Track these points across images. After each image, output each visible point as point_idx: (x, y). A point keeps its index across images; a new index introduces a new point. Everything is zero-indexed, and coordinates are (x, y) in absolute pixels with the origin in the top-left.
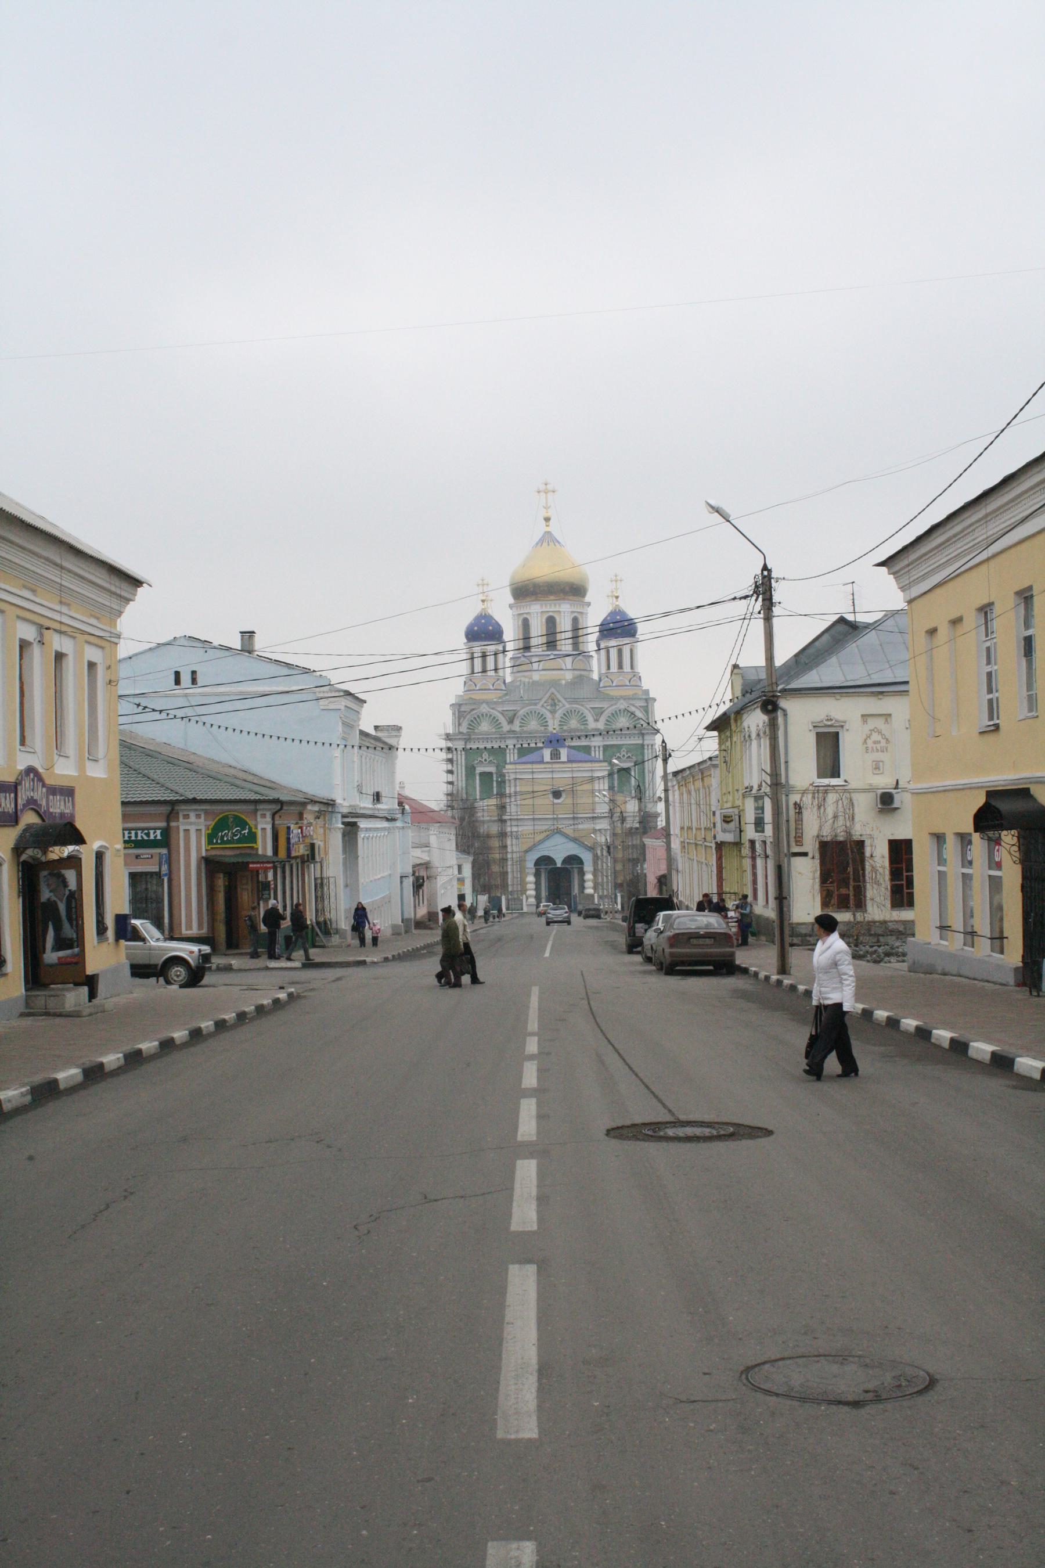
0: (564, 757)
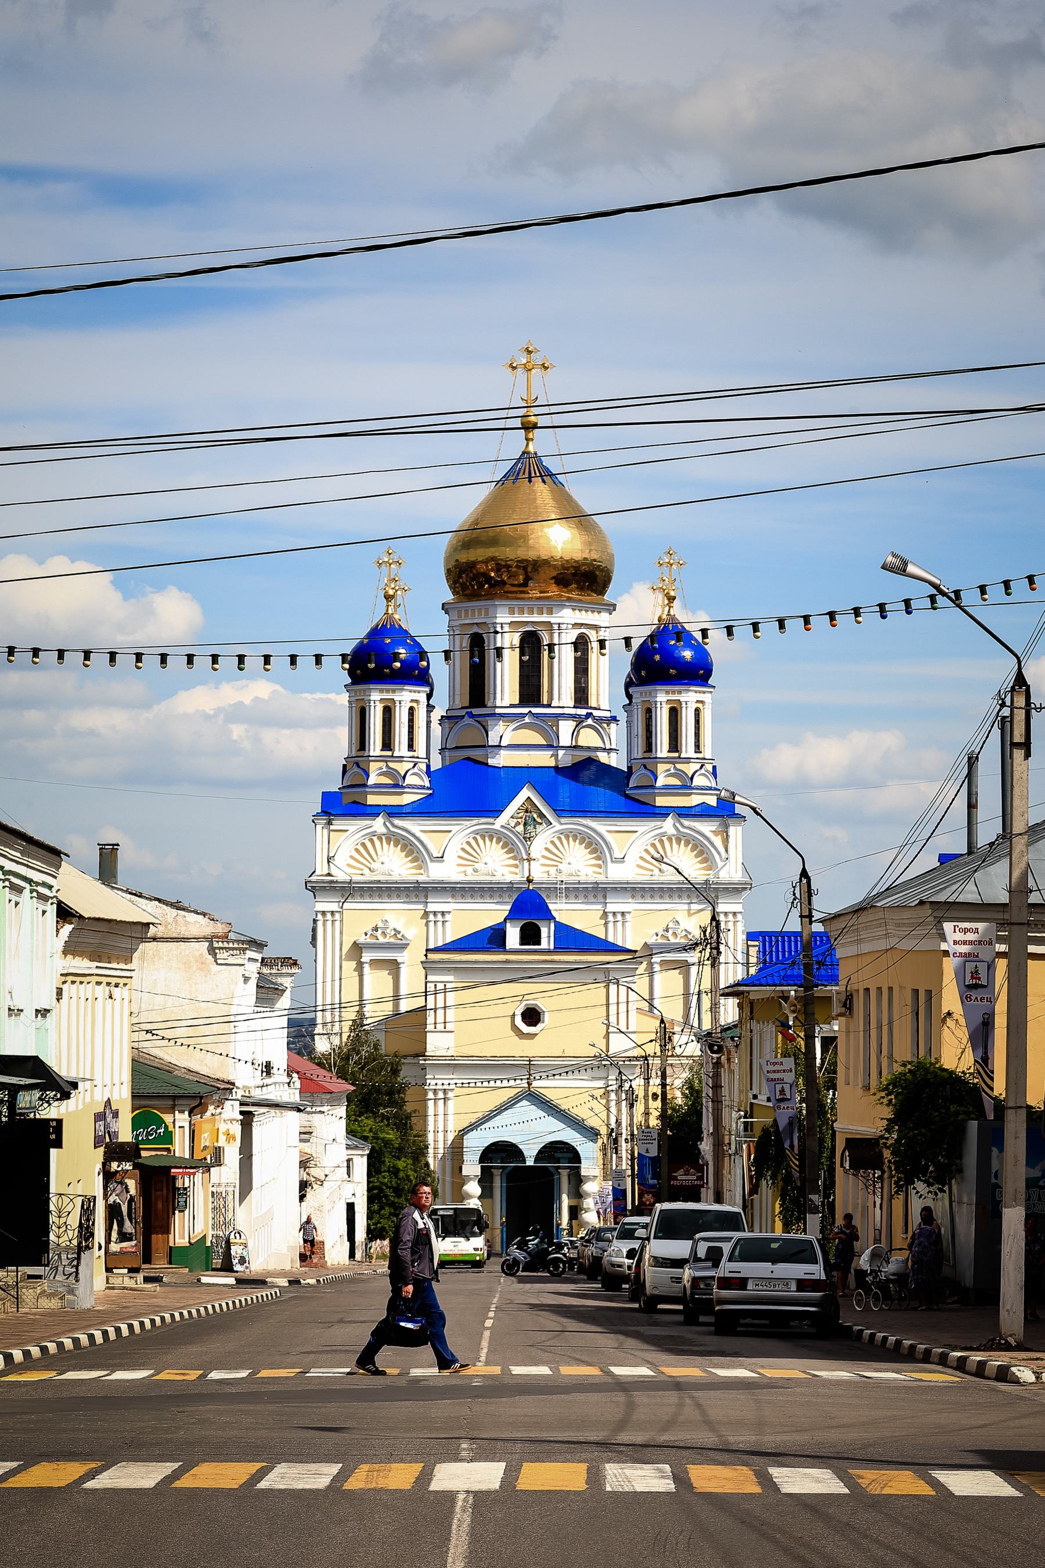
0: (547, 939)
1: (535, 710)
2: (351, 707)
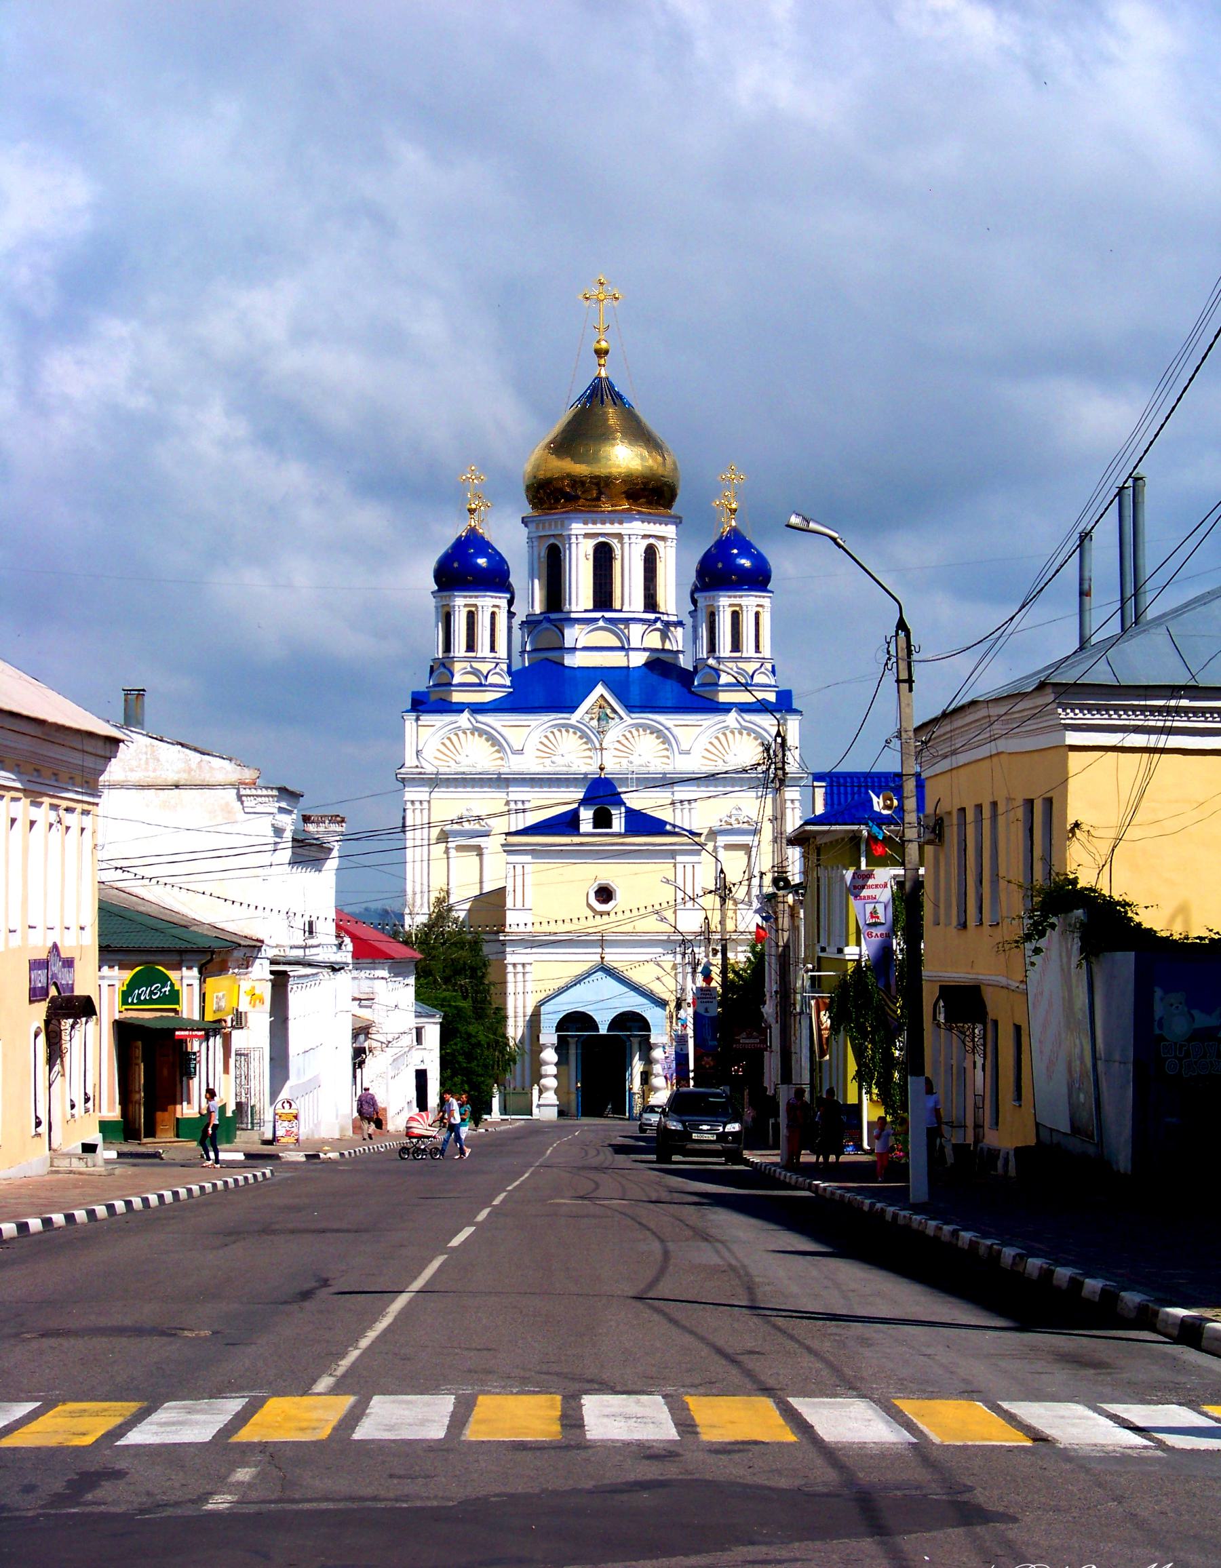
0: (618, 824)
1: (608, 615)
2: (437, 612)
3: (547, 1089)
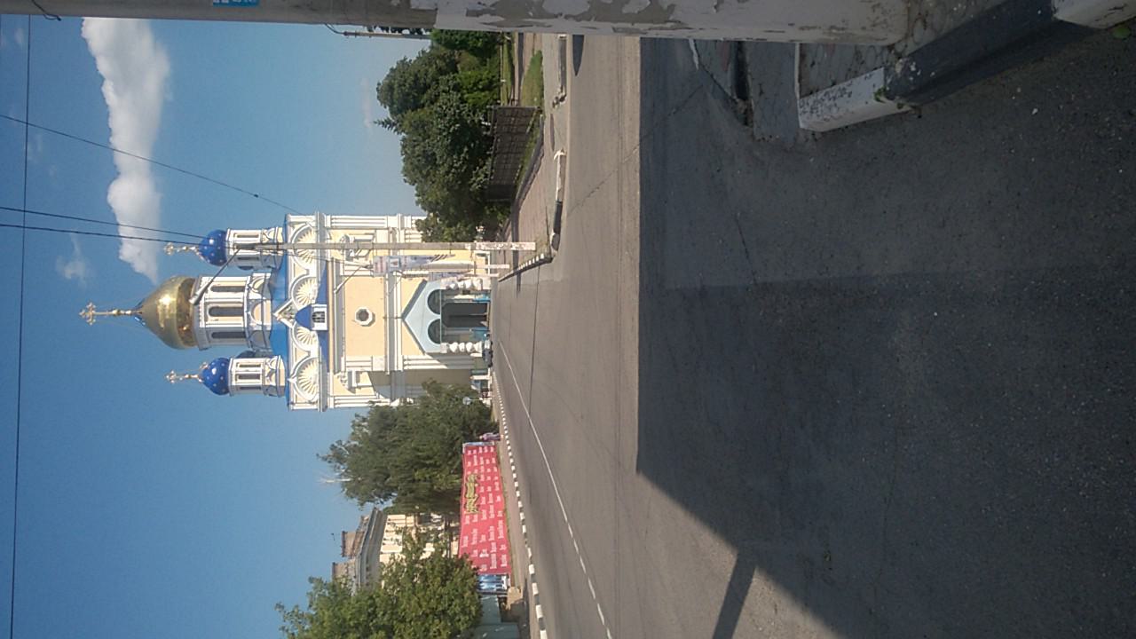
1: (245, 309)
3: (473, 348)
